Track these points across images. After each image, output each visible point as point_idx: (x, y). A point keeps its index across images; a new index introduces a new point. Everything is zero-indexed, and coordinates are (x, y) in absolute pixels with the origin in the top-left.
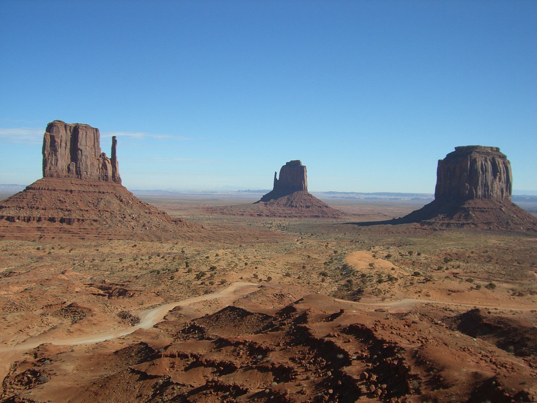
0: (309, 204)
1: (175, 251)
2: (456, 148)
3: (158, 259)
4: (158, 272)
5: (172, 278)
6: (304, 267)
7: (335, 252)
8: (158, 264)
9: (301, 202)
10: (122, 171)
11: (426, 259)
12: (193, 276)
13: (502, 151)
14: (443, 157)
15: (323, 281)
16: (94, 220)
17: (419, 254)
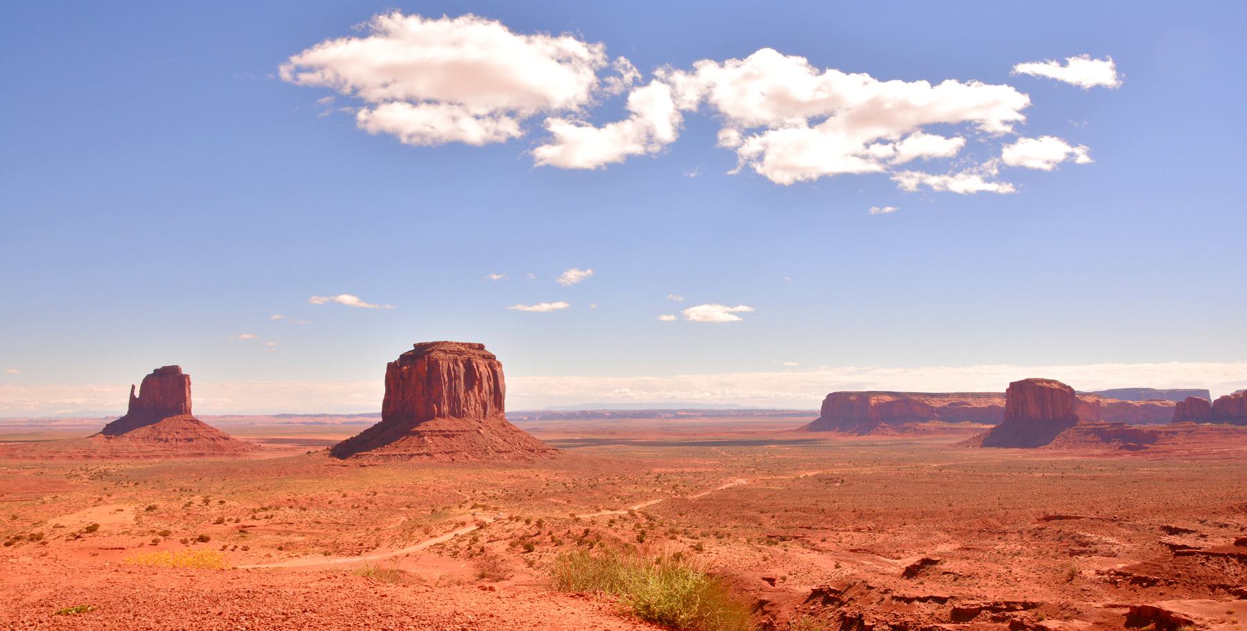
0: (190, 436)
2: (414, 345)
9: (177, 433)
14: (395, 358)
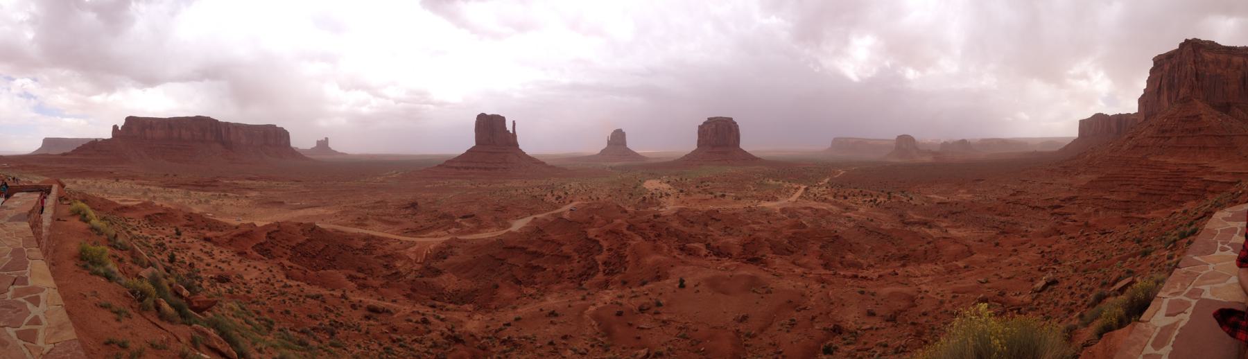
1: (548, 184)
3: (538, 189)
4: (536, 197)
5: (543, 200)
6: (620, 191)
7: (640, 181)
8: (537, 192)
10: (520, 140)
11: (690, 182)
12: (554, 198)
13: (735, 120)
14: (701, 124)
15: (630, 198)
16: (504, 168)
17: (686, 179)
